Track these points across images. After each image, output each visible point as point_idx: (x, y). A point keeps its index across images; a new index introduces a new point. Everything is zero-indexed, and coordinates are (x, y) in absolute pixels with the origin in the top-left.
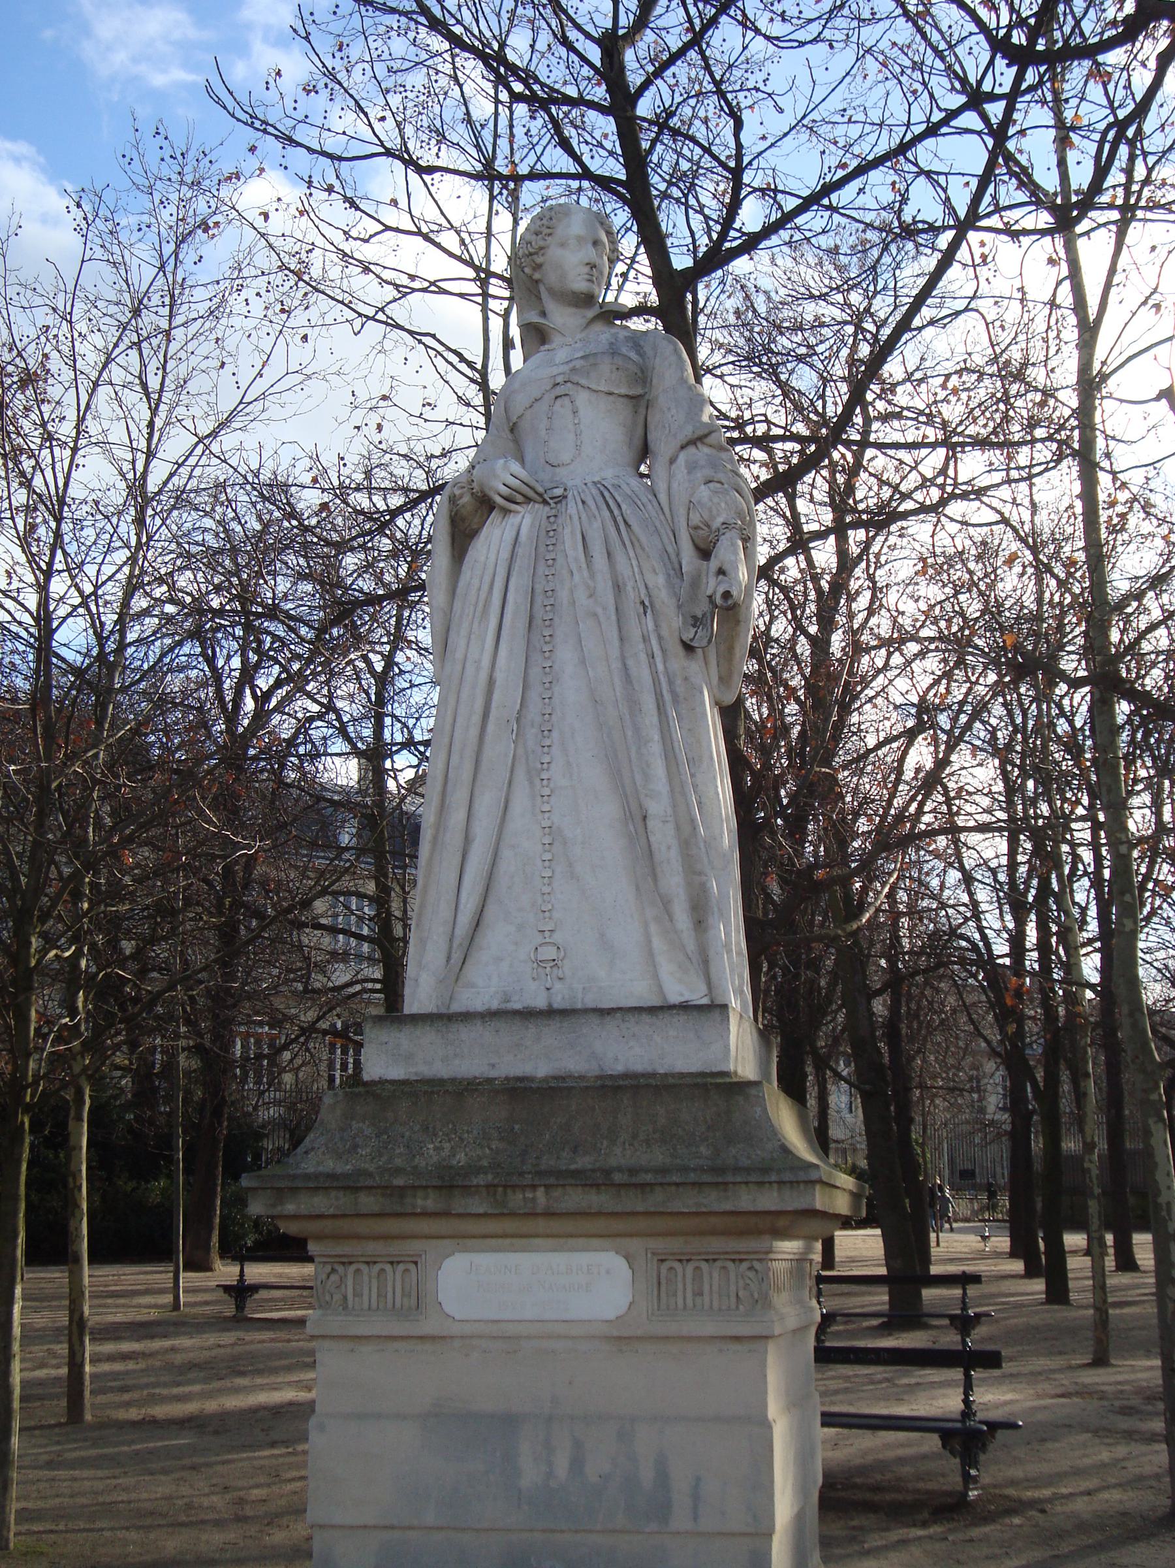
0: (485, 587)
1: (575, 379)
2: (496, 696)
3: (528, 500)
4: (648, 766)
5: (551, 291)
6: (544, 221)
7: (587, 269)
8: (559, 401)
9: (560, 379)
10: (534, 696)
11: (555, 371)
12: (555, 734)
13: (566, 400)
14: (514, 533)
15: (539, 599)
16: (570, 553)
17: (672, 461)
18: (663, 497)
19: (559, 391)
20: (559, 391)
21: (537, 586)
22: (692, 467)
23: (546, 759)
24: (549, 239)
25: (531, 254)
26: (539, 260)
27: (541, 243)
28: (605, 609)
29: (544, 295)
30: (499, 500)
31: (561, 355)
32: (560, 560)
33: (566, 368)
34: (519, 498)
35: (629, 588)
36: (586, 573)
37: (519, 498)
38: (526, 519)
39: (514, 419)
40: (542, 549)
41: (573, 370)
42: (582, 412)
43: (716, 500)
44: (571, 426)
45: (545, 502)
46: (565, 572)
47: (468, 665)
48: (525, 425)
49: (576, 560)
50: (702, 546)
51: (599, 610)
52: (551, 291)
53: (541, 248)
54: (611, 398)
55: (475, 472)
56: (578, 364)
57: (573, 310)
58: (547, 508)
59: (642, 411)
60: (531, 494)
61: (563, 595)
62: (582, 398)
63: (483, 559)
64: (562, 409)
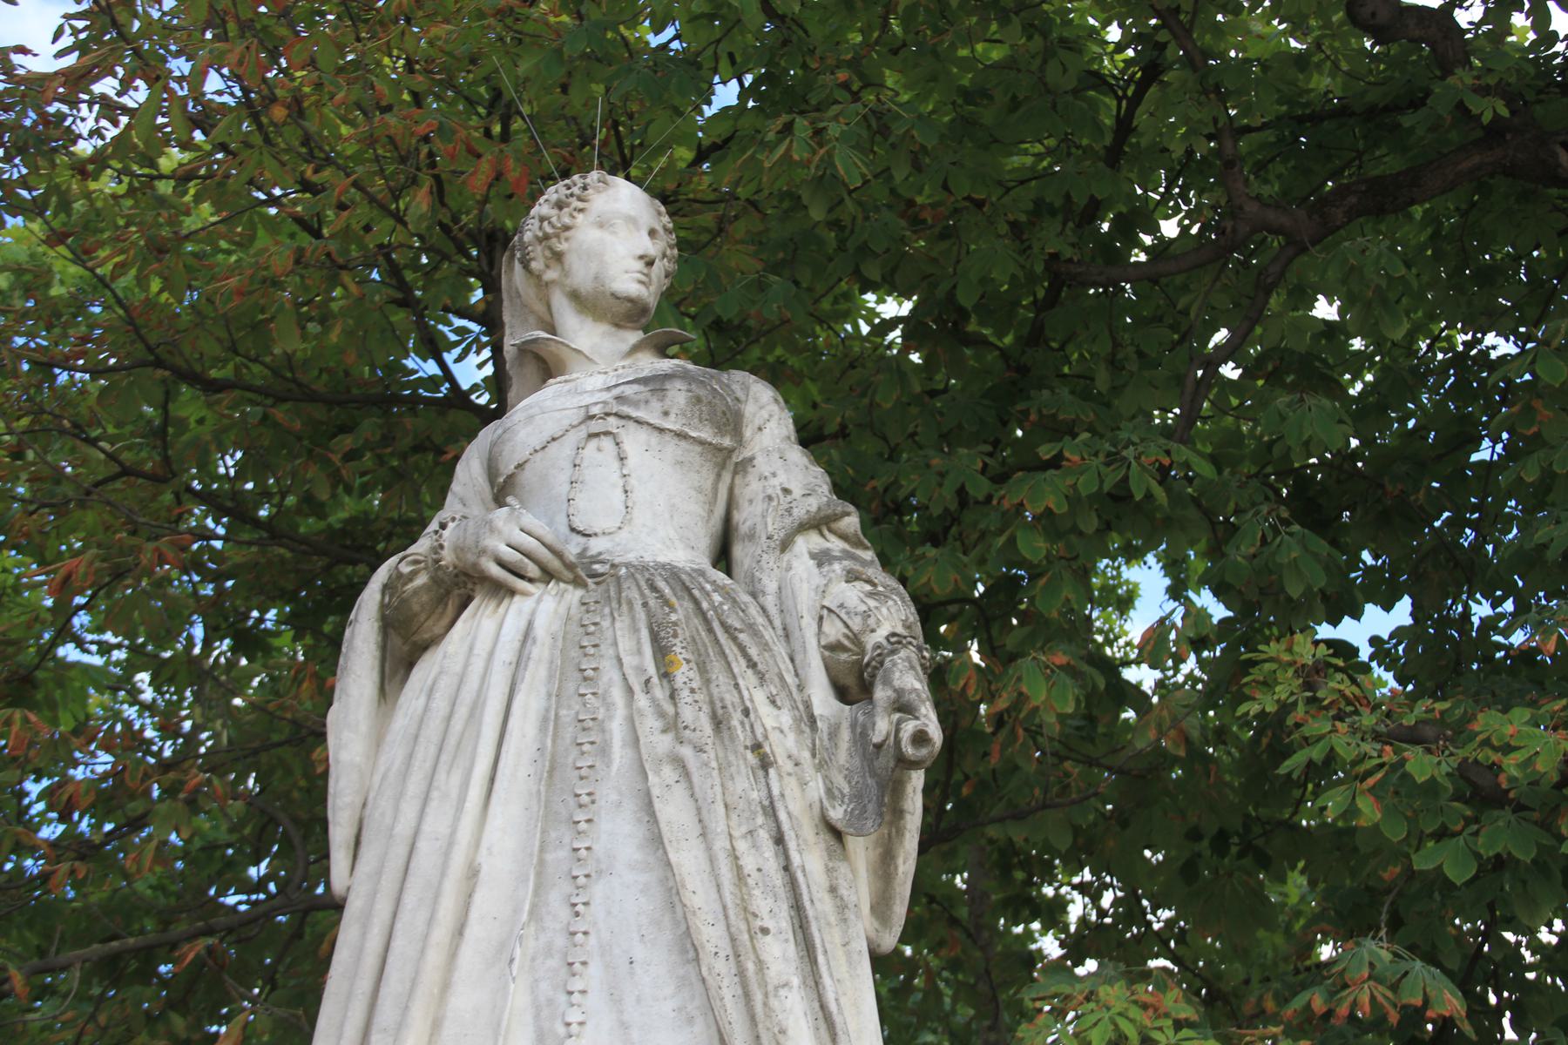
0: (462, 711)
1: (626, 410)
2: (478, 898)
3: (548, 575)
4: (783, 1032)
5: (575, 296)
6: (576, 190)
7: (640, 265)
8: (594, 443)
9: (595, 410)
10: (555, 900)
11: (587, 400)
12: (595, 970)
13: (607, 443)
14: (523, 624)
15: (568, 733)
16: (628, 661)
17: (785, 545)
18: (770, 601)
19: (595, 426)
20: (595, 426)
21: (563, 712)
22: (822, 559)
23: (574, 1016)
24: (580, 217)
25: (547, 237)
26: (562, 246)
27: (567, 220)
28: (700, 750)
29: (560, 303)
30: (495, 570)
31: (598, 381)
32: (610, 674)
33: (606, 396)
34: (533, 570)
35: (735, 723)
36: (660, 693)
37: (533, 570)
38: (545, 607)
39: (507, 467)
40: (575, 653)
41: (618, 398)
42: (632, 462)
43: (872, 603)
44: (615, 478)
45: (577, 582)
46: (617, 695)
47: (422, 845)
48: (527, 476)
49: (641, 670)
50: (850, 681)
51: (686, 752)
52: (575, 296)
53: (567, 228)
54: (683, 444)
55: (446, 533)
56: (629, 390)
57: (604, 328)
58: (579, 593)
59: (727, 477)
60: (555, 564)
61: (617, 729)
62: (635, 441)
63: (457, 667)
64: (599, 456)
